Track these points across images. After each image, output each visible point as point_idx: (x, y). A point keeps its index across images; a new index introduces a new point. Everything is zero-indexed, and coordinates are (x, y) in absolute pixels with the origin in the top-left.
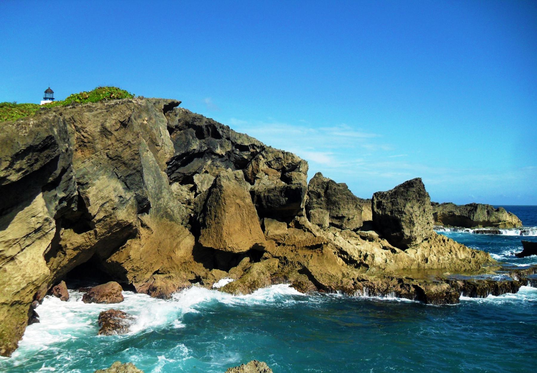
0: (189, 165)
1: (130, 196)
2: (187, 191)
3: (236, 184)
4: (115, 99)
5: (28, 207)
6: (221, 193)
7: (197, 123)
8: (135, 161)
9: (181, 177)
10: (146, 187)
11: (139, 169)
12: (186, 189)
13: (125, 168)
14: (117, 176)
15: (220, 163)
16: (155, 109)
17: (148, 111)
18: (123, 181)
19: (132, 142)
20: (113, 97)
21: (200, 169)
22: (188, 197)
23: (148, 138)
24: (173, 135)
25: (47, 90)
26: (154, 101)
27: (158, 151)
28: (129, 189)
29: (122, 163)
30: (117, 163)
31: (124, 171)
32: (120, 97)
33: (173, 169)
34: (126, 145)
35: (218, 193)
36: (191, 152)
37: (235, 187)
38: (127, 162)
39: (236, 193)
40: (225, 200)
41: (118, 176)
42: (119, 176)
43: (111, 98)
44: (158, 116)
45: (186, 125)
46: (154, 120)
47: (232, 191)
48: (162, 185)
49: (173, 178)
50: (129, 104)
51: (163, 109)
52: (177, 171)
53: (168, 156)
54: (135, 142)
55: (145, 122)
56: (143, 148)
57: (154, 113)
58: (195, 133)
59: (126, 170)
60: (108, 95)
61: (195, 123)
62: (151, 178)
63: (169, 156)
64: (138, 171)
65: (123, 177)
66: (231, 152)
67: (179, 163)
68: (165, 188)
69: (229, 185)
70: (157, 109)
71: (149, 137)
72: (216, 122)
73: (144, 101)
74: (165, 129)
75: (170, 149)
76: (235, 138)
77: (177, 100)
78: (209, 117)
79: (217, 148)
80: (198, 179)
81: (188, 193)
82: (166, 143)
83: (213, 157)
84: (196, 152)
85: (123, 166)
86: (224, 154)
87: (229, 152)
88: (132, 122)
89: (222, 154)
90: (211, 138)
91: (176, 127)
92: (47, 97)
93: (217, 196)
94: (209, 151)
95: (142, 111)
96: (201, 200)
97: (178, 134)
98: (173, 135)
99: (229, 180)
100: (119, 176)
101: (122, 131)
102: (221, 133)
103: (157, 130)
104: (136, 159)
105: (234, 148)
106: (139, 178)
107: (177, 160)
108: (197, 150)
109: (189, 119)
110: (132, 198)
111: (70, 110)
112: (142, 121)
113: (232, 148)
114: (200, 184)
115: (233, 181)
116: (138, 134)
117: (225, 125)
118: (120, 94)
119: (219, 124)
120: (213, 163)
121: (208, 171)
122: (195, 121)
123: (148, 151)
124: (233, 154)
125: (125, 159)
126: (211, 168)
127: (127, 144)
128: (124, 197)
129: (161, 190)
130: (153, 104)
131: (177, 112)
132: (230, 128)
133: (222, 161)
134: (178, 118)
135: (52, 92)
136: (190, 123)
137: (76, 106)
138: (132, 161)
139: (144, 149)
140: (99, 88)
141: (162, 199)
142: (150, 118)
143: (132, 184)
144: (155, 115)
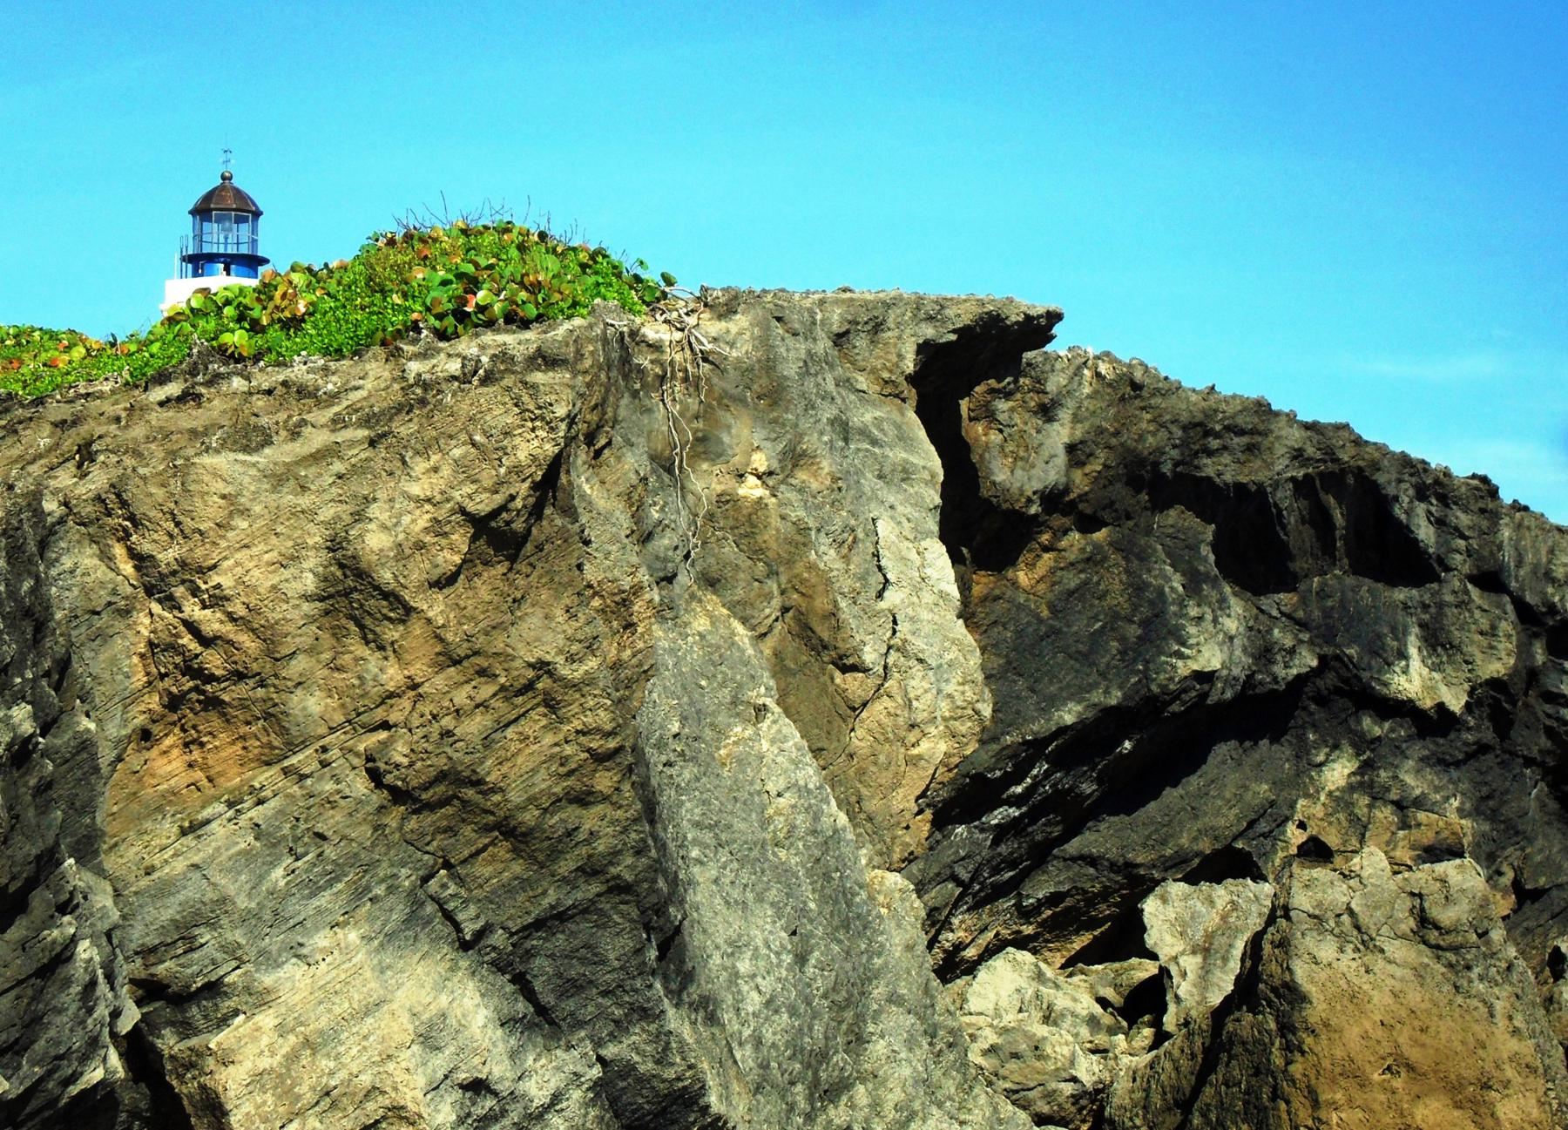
0: (1171, 795)
1: (556, 1081)
2: (1093, 1021)
3: (1419, 973)
4: (490, 324)
5: (1179, 791)
6: (1288, 1048)
7: (1222, 469)
8: (598, 809)
9: (1105, 895)
10: (707, 1009)
11: (625, 869)
12: (1088, 1005)
13: (517, 868)
14: (448, 929)
15: (1429, 774)
16: (845, 383)
17: (774, 404)
18: (499, 966)
19: (565, 671)
20: (482, 309)
21: (1263, 826)
22: (1088, 1070)
23: (771, 610)
24: (1031, 566)
25: (208, 197)
26: (836, 318)
27: (856, 709)
28: (552, 1023)
29: (487, 829)
30: (450, 831)
31: (508, 890)
32: (532, 311)
33: (1039, 832)
34: (521, 692)
35: (1266, 1051)
36: (1176, 696)
37: (1414, 997)
38: (529, 817)
39: (1414, 1054)
40: (1316, 1104)
41: (457, 927)
42: (469, 930)
43: (461, 316)
44: (864, 433)
45: (1135, 483)
46: (826, 465)
47: (1379, 1033)
48: (870, 977)
49: (1041, 904)
50: (538, 377)
51: (911, 379)
52: (1073, 846)
53: (935, 747)
54: (592, 663)
55: (752, 489)
56: (725, 694)
57: (827, 412)
58: (1215, 547)
59: (525, 883)
60: (443, 298)
61: (1209, 467)
62: (766, 930)
63: (943, 747)
64: (619, 889)
65: (498, 938)
66: (1518, 687)
67: (1088, 788)
68: (894, 999)
69: (1364, 982)
70: (862, 382)
71: (776, 602)
72: (1381, 448)
73: (740, 322)
74: (919, 534)
75: (950, 688)
76: (1549, 577)
77: (1031, 300)
78: (1326, 417)
79: (1403, 655)
80: (1182, 928)
81: (1101, 1039)
82: (918, 644)
83: (1370, 726)
84: (1221, 693)
85: (502, 850)
86: (1456, 701)
87: (1494, 683)
88: (570, 512)
89: (1441, 707)
90: (1350, 581)
91: (1053, 499)
92: (207, 249)
93: (1257, 1073)
94: (1331, 679)
95: (726, 400)
96: (1157, 1100)
97: (1072, 556)
98: (1031, 566)
99: (1367, 943)
100: (469, 930)
101: (487, 585)
102: (1425, 533)
103: (847, 544)
104: (606, 798)
105: (1540, 655)
106: (626, 943)
107: (1060, 761)
108: (1230, 681)
109: (1149, 437)
110: (576, 1095)
111: (157, 417)
112: (728, 483)
113: (1523, 651)
114: (1191, 963)
115: (1395, 949)
116: (625, 603)
117: (1461, 470)
118: (534, 288)
119: (1405, 461)
120: (1365, 783)
121: (1332, 839)
122: (1210, 453)
123: (761, 710)
124: (1532, 698)
125: (515, 797)
126: (1354, 820)
127: (529, 687)
128: (503, 1088)
129: (860, 1018)
130: (823, 345)
131: (1057, 381)
132: (1506, 497)
133: (1442, 763)
134: (1060, 433)
135: (247, 212)
136: (1166, 469)
137: (209, 383)
138: (571, 813)
139: (735, 702)
140: (391, 242)
141: (861, 1093)
142: (794, 458)
143: (572, 987)
144: (843, 429)
